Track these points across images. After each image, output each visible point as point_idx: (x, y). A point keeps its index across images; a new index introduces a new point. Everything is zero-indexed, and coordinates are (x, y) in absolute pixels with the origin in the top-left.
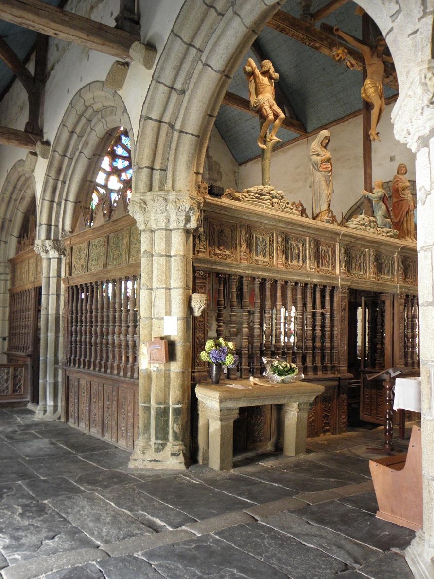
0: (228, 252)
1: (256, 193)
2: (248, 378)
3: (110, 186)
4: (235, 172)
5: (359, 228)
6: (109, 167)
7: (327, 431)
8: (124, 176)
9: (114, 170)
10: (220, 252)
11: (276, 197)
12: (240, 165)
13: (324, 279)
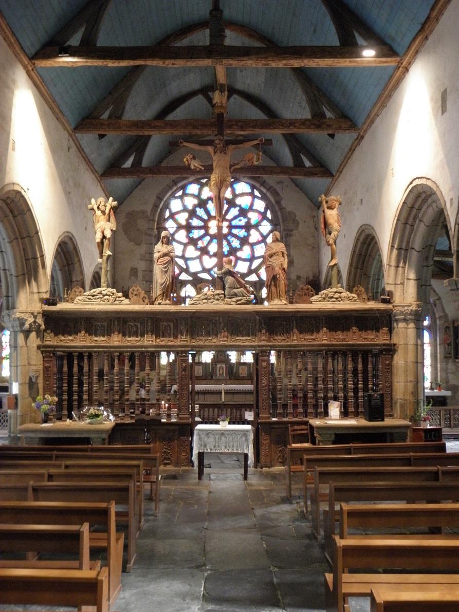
0: (71, 338)
1: (89, 295)
2: (66, 421)
3: (187, 256)
4: (314, 217)
5: (198, 303)
6: (186, 238)
7: (168, 464)
8: (200, 244)
10: (64, 339)
11: (106, 295)
13: (155, 348)
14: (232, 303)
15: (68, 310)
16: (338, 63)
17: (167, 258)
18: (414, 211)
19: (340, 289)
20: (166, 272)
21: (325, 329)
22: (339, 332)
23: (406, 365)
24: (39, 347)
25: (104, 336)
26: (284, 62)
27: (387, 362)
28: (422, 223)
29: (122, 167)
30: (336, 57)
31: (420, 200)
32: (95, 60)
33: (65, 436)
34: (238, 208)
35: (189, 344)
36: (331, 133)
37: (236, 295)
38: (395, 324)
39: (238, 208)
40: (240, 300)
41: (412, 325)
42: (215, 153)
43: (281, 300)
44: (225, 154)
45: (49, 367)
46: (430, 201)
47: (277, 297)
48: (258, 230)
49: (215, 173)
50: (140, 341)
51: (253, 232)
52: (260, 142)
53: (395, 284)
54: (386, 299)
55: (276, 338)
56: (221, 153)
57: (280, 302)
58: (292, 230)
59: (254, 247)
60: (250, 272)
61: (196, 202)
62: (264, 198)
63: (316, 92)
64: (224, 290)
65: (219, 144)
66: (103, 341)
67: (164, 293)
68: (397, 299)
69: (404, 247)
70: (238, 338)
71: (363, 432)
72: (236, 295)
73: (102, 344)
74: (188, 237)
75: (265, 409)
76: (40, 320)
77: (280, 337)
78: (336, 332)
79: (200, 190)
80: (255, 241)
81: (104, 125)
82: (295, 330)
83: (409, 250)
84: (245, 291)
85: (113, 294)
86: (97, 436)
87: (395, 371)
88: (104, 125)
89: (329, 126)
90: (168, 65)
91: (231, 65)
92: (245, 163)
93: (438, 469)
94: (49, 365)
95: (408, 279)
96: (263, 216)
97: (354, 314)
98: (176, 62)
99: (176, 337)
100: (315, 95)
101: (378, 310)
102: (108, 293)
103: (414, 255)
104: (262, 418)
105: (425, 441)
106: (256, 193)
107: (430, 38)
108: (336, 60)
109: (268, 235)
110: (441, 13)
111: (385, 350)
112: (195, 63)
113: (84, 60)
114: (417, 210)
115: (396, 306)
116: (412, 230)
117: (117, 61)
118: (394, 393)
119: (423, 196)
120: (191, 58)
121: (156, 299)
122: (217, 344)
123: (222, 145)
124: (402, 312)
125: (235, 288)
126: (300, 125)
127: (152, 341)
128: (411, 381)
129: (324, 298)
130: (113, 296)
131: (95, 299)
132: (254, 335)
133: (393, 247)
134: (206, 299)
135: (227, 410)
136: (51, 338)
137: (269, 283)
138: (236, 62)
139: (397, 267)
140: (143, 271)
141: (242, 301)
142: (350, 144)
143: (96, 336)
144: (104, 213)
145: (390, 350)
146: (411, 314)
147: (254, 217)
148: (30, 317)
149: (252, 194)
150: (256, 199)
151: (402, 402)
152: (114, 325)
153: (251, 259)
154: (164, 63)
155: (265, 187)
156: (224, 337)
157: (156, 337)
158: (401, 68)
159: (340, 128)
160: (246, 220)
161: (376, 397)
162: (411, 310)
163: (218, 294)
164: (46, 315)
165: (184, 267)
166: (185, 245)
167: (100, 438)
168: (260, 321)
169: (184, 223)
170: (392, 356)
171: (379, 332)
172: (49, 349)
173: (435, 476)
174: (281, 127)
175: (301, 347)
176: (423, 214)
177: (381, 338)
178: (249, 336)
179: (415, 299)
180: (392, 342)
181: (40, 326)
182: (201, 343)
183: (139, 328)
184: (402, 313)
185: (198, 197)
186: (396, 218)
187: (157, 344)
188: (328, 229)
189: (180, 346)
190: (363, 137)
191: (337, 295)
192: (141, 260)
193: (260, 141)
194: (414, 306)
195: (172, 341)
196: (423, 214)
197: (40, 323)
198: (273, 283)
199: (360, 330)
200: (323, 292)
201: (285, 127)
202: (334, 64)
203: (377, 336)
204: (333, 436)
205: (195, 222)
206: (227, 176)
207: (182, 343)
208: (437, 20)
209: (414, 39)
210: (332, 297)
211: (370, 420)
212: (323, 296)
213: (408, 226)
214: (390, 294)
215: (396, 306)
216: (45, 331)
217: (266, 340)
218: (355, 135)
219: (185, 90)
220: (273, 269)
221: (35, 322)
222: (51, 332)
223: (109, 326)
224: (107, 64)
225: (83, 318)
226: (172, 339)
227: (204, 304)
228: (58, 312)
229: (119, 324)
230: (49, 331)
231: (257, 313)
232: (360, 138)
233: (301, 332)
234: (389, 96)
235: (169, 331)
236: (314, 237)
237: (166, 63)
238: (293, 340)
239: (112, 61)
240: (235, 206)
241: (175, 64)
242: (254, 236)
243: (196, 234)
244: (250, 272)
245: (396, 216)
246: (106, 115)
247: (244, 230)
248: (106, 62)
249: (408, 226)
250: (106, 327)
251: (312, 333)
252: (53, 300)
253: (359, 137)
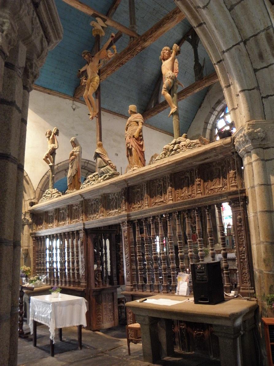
40: (106, 176)
82: (146, 195)
125: (103, 167)
135: (86, 283)
141: (107, 177)
161: (200, 268)
175: (149, 212)
197: (28, 219)
210: (172, 150)
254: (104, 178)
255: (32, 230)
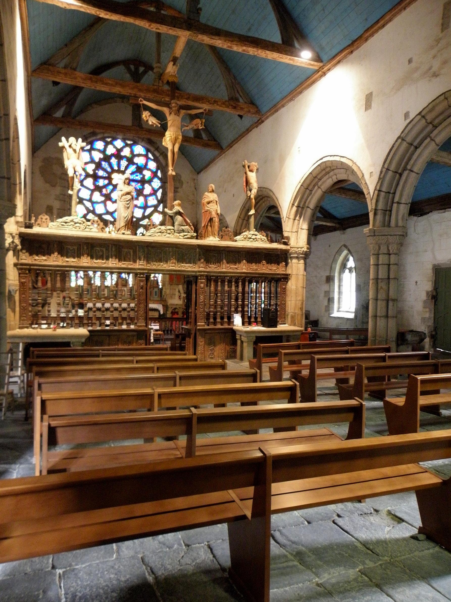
0: (44, 258)
1: (62, 222)
4: (194, 180)
9: (97, 188)
11: (78, 223)
12: (198, 173)
14: (180, 237)
15: (44, 233)
16: (281, 58)
17: (129, 197)
18: (316, 180)
19: (256, 233)
20: (128, 208)
21: (244, 261)
22: (254, 264)
23: (297, 289)
24: (15, 265)
25: (74, 258)
26: (244, 48)
27: (284, 287)
28: (320, 189)
29: (54, 116)
30: (281, 53)
31: (324, 172)
32: (90, 7)
33: (49, 341)
34: (135, 166)
35: (145, 267)
36: (241, 114)
37: (183, 231)
38: (290, 260)
39: (135, 166)
41: (302, 261)
42: (170, 114)
43: (215, 237)
44: (178, 116)
45: (25, 282)
46: (331, 173)
47: (212, 235)
48: (150, 185)
49: (170, 131)
50: (105, 263)
51: (146, 186)
52: (204, 111)
53: (292, 232)
54: (286, 242)
55: (210, 266)
56: (175, 115)
57: (214, 239)
58: (178, 188)
59: (147, 198)
60: (144, 217)
61: (102, 156)
62: (156, 160)
63: (233, 81)
64: (173, 226)
65: (175, 107)
66: (73, 262)
67: (126, 225)
68: (292, 242)
69: (301, 206)
70: (182, 265)
71: (274, 334)
72: (183, 231)
73: (72, 264)
74: (94, 184)
75: (202, 319)
76: (17, 241)
77: (213, 266)
78: (251, 264)
79: (106, 147)
80: (148, 193)
81: (61, 73)
82: (225, 261)
83: (305, 209)
84: (190, 229)
85: (84, 222)
86: (77, 340)
87: (288, 293)
88: (61, 73)
89: (242, 109)
90: (152, 28)
91: (203, 40)
92: (193, 126)
93: (386, 355)
94: (24, 280)
95: (301, 229)
96: (154, 175)
97: (264, 251)
98: (160, 28)
99: (135, 261)
100: (232, 83)
101: (280, 249)
102: (80, 222)
103: (309, 212)
104: (199, 326)
105: (310, 341)
106: (150, 155)
107: (354, 53)
108: (281, 55)
109: (158, 189)
110: (372, 35)
111: (283, 278)
112: (175, 32)
113: (80, 5)
114: (319, 179)
115: (292, 248)
116: (311, 193)
117: (110, 14)
118: (287, 309)
119: (328, 170)
120: (174, 27)
121: (119, 229)
122: (167, 268)
123: (177, 108)
124: (296, 252)
126: (222, 104)
127: (116, 264)
128: (299, 300)
129: (245, 238)
130: (84, 224)
131: (68, 225)
132: (195, 263)
133: (293, 205)
134: (160, 232)
136: (26, 257)
137: (206, 224)
138: (209, 39)
139: (295, 219)
140: (59, 209)
141: (188, 236)
142: (249, 126)
143: (67, 257)
144: (75, 151)
145: (286, 278)
146: (302, 254)
147: (147, 174)
148: (9, 237)
149: (146, 156)
150: (149, 160)
151: (293, 314)
152: (83, 249)
153: (145, 207)
154: (150, 26)
155: (159, 152)
156: (172, 263)
157: (119, 261)
158: (320, 72)
159: (249, 112)
160: (142, 176)
162: (303, 251)
163: (170, 230)
164: (22, 236)
165: (91, 209)
166: (93, 191)
167: (79, 342)
168: (199, 253)
169: (91, 173)
170: (287, 282)
171: (279, 265)
172: (25, 267)
173: (383, 359)
174: (207, 103)
176: (323, 183)
177: (281, 270)
178: (191, 264)
179: (306, 243)
180: (287, 273)
181: (17, 246)
182: (154, 267)
183: (105, 253)
184: (296, 253)
185: (103, 152)
186: (300, 184)
187: (119, 266)
188: (249, 186)
189: (139, 269)
190: (263, 122)
191: (254, 237)
192: (56, 199)
193: (204, 110)
194: (306, 248)
195: (131, 265)
196: (323, 183)
198: (209, 224)
199: (267, 263)
200: (244, 233)
201: (210, 103)
202: (277, 58)
203: (278, 268)
204: (255, 338)
205: (101, 173)
206: (179, 135)
207: (140, 267)
208: (366, 40)
209: (341, 51)
210: (250, 238)
211: (269, 327)
212: (245, 237)
213: (308, 191)
214: (288, 238)
215: (292, 248)
216: (21, 250)
217: (204, 268)
218: (255, 118)
219: (113, 57)
220: (210, 213)
221: (13, 242)
222: (27, 252)
223: (79, 249)
224: (99, 14)
225: (56, 241)
226: (132, 263)
227: (159, 236)
228: (34, 235)
229: (87, 248)
230: (24, 251)
231: (199, 246)
232: (260, 122)
233: (228, 263)
234: (301, 92)
235: (129, 257)
236: (194, 195)
237: (152, 27)
238: (223, 268)
239: (105, 12)
240: (134, 164)
241: (159, 29)
242: (147, 190)
243: (101, 183)
244: (144, 217)
245: (300, 182)
246: (62, 65)
247: (140, 184)
248: (99, 11)
249: (308, 191)
250: (76, 250)
251: (235, 263)
252: (30, 224)
253: (260, 121)
254: (185, 236)
255: (18, 259)
